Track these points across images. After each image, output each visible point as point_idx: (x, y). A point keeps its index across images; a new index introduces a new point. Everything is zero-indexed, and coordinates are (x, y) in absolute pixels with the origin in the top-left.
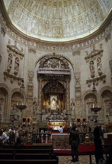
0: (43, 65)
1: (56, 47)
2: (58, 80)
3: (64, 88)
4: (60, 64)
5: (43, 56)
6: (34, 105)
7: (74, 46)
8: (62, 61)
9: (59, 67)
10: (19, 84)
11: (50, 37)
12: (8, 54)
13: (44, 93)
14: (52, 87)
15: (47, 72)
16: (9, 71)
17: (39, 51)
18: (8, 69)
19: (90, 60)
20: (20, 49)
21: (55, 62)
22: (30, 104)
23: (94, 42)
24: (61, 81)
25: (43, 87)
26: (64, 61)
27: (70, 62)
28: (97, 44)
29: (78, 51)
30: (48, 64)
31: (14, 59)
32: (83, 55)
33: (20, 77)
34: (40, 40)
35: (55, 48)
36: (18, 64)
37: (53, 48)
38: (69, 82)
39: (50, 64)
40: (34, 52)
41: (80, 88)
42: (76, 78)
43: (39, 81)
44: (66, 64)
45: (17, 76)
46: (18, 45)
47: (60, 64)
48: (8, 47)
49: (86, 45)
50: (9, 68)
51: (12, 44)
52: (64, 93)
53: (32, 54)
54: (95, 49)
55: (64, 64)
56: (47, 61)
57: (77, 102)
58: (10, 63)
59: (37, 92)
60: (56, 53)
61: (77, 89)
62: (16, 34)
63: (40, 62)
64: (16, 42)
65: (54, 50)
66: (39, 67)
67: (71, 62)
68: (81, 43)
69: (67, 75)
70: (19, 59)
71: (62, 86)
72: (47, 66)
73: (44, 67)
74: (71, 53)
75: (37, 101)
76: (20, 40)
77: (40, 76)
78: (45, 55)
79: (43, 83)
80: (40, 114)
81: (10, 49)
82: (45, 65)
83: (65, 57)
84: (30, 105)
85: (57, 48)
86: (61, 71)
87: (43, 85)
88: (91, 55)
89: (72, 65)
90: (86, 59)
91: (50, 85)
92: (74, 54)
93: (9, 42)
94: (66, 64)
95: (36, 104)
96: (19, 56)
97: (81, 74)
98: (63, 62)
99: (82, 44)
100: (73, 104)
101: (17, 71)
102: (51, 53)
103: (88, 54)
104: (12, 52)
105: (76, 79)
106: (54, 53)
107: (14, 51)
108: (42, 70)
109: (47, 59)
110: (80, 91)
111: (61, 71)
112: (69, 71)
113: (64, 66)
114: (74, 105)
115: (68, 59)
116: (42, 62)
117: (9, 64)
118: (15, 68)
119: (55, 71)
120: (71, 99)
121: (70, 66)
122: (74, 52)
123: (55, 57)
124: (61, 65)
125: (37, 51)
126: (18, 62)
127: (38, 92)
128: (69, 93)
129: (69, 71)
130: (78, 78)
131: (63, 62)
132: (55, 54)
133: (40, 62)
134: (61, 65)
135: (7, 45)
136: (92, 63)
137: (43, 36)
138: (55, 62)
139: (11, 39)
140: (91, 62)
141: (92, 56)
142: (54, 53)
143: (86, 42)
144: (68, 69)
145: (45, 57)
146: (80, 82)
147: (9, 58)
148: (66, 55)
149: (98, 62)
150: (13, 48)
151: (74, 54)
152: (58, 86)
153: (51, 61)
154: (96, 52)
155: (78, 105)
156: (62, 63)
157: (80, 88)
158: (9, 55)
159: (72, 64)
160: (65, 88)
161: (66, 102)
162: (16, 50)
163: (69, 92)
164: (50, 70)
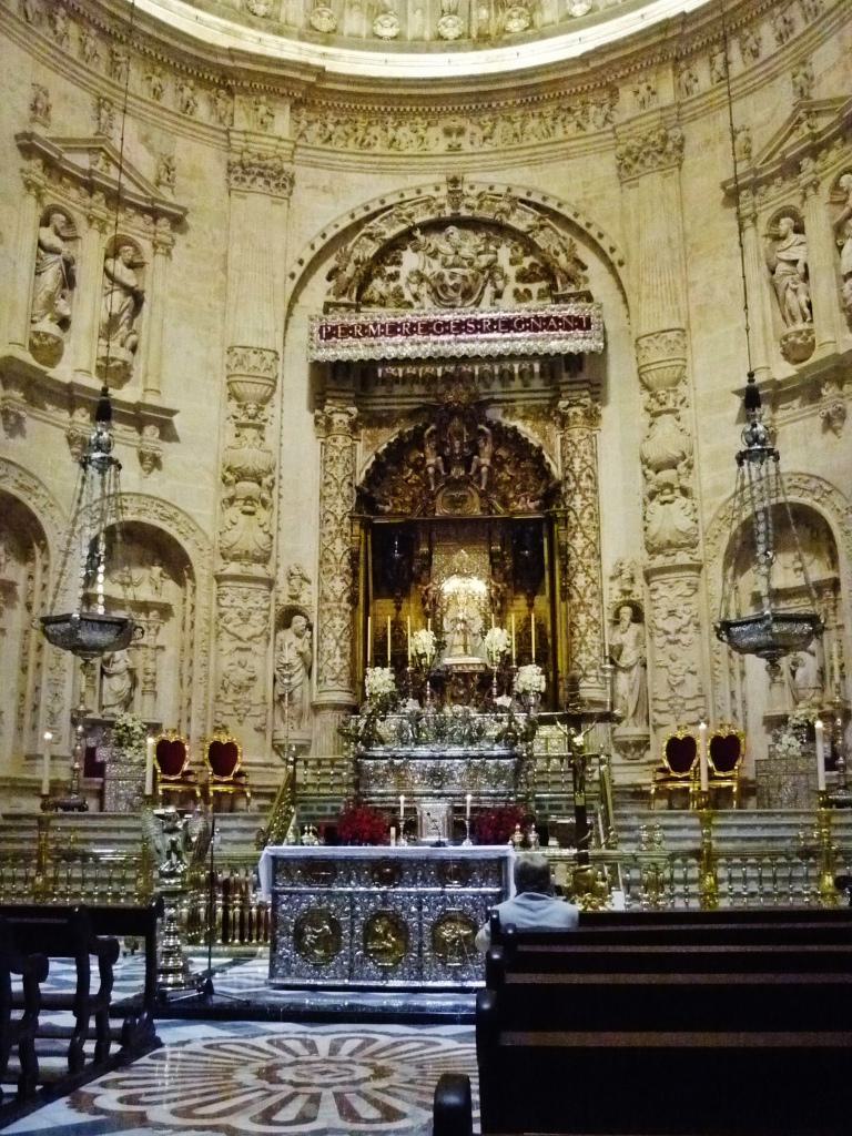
0: (362, 288)
1: (470, 128)
2: (494, 414)
3: (543, 472)
5: (361, 214)
6: (287, 636)
7: (626, 94)
8: (526, 242)
9: (498, 295)
10: (142, 457)
11: (417, 46)
12: (33, 212)
13: (367, 525)
14: (437, 470)
15: (391, 347)
16: (50, 351)
17: (325, 176)
18: (37, 334)
19: (779, 195)
20: (146, 165)
21: (466, 252)
22: (246, 620)
23: (800, 27)
24: (524, 418)
25: (360, 478)
26: (541, 240)
27: (594, 245)
28: (834, 39)
29: (665, 139)
30: (401, 282)
31: (90, 251)
32: (708, 168)
33: (151, 400)
34: (321, 73)
35: (461, 132)
36: (137, 298)
37: (448, 133)
38: (592, 417)
39: (422, 279)
40: (279, 180)
41: (690, 466)
42: (651, 378)
43: (326, 426)
44: (562, 259)
45: (127, 394)
46: (127, 136)
47: (511, 271)
48: (27, 146)
49: (737, 68)
50: (47, 326)
51: (72, 119)
52: (551, 521)
53: (257, 202)
54: (820, 93)
55: (547, 272)
56: (390, 250)
57: (663, 590)
58: (51, 277)
59: (315, 521)
60: (470, 177)
61: (667, 475)
62: (104, 34)
63: (331, 263)
64: (101, 103)
65: (454, 149)
66: (326, 311)
67: (604, 244)
68: (690, 56)
69: (574, 362)
70: (137, 250)
71: (529, 458)
72: (398, 294)
73: (369, 303)
74: (604, 166)
75: (309, 598)
76: (146, 95)
77: (331, 380)
78: (375, 207)
79: (360, 446)
80: (336, 707)
81: (50, 165)
82: (378, 286)
83: (551, 204)
84: (245, 635)
85: (477, 129)
86: (508, 325)
87: (364, 460)
88: (778, 156)
89: (610, 265)
90: (732, 195)
91: (424, 460)
92: (629, 165)
93: (39, 109)
94: (562, 259)
95: (299, 621)
96: (73, 193)
97: (698, 339)
98: (530, 247)
99: (703, 75)
100: (626, 612)
101: (123, 354)
102: (430, 182)
103: (754, 154)
104: (72, 199)
105: (647, 387)
106: (454, 181)
107: (91, 187)
108: (348, 331)
109: (390, 234)
110: (685, 492)
111: (508, 325)
113: (543, 285)
114: (638, 616)
115: (581, 222)
116: (351, 269)
117: (42, 297)
118: (111, 325)
119: (461, 327)
120: (608, 568)
121: (597, 279)
122: (629, 153)
123: (464, 212)
124: (522, 277)
126: (128, 277)
127: (324, 521)
128: (595, 516)
129: (581, 324)
130: (669, 375)
131: (530, 247)
132: (466, 189)
133: (331, 263)
134: (522, 277)
135: (17, 137)
136: (786, 224)
137: (356, 43)
138: (466, 252)
139: (58, 85)
140: (776, 221)
141: (792, 168)
142: (454, 181)
143: (734, 45)
144: (572, 309)
145: (375, 215)
146: (683, 412)
147: (40, 245)
148: (557, 183)
149: (837, 208)
150: (82, 161)
151: (629, 165)
152: (497, 463)
153: (434, 255)
154: (822, 123)
155: (672, 613)
156: (527, 262)
157: (681, 465)
158: (45, 222)
159: (614, 258)
160: (557, 472)
161: (566, 596)
162: (114, 173)
163: (595, 504)
164: (413, 328)
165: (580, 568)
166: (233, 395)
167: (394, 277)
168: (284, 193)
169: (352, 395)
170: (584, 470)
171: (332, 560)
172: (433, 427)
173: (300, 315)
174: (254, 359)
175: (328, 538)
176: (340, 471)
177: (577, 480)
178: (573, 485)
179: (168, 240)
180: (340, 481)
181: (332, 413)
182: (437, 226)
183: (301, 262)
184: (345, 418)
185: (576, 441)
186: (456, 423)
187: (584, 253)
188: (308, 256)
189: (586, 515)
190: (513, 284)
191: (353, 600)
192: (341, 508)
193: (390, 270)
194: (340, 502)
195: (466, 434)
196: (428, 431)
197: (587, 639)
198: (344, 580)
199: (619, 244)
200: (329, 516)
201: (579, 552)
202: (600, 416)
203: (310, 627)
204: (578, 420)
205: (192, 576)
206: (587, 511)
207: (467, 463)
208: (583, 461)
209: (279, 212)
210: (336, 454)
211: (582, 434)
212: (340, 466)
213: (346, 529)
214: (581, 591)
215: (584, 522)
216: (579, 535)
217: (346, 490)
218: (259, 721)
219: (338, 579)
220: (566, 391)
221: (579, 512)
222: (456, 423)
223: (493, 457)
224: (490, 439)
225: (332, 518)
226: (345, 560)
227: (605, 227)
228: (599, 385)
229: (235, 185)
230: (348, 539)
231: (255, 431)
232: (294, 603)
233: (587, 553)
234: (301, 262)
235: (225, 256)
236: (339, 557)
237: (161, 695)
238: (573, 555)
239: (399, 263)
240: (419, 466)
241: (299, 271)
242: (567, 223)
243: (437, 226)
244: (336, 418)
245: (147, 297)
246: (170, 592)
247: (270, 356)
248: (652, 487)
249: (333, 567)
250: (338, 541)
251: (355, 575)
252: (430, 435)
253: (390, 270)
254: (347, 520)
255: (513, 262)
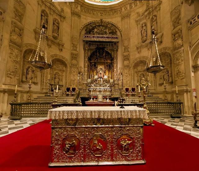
2: (106, 49)
4: (108, 32)
17: (85, 17)
38: (117, 50)
41: (129, 56)
44: (114, 31)
47: (108, 32)
67: (119, 29)
75: (83, 70)
79: (89, 53)
100: (120, 74)
112: (117, 38)
115: (117, 26)
123: (102, 24)
125: (82, 16)
129: (117, 38)
133: (85, 29)
152: (106, 56)
156: (110, 31)
160: (113, 57)
166: (72, 44)
167: (94, 32)
168: (79, 18)
173: (82, 35)
174: (75, 39)
179: (63, 20)
182: (99, 26)
183: (82, 28)
187: (117, 30)
188: (83, 27)
190: (108, 34)
191: (88, 71)
192: (86, 59)
193: (93, 31)
199: (121, 28)
203: (82, 74)
205: (67, 66)
207: (102, 55)
209: (79, 20)
218: (76, 85)
223: (105, 55)
227: (119, 26)
229: (73, 15)
234: (82, 28)
235: (71, 25)
237: (63, 81)
239: (94, 30)
240: (97, 55)
241: (81, 29)
242: (115, 26)
243: (99, 26)
244: (86, 48)
245: (60, 27)
246: (64, 68)
247: (77, 39)
251: (88, 68)
253: (93, 31)
255: (108, 31)
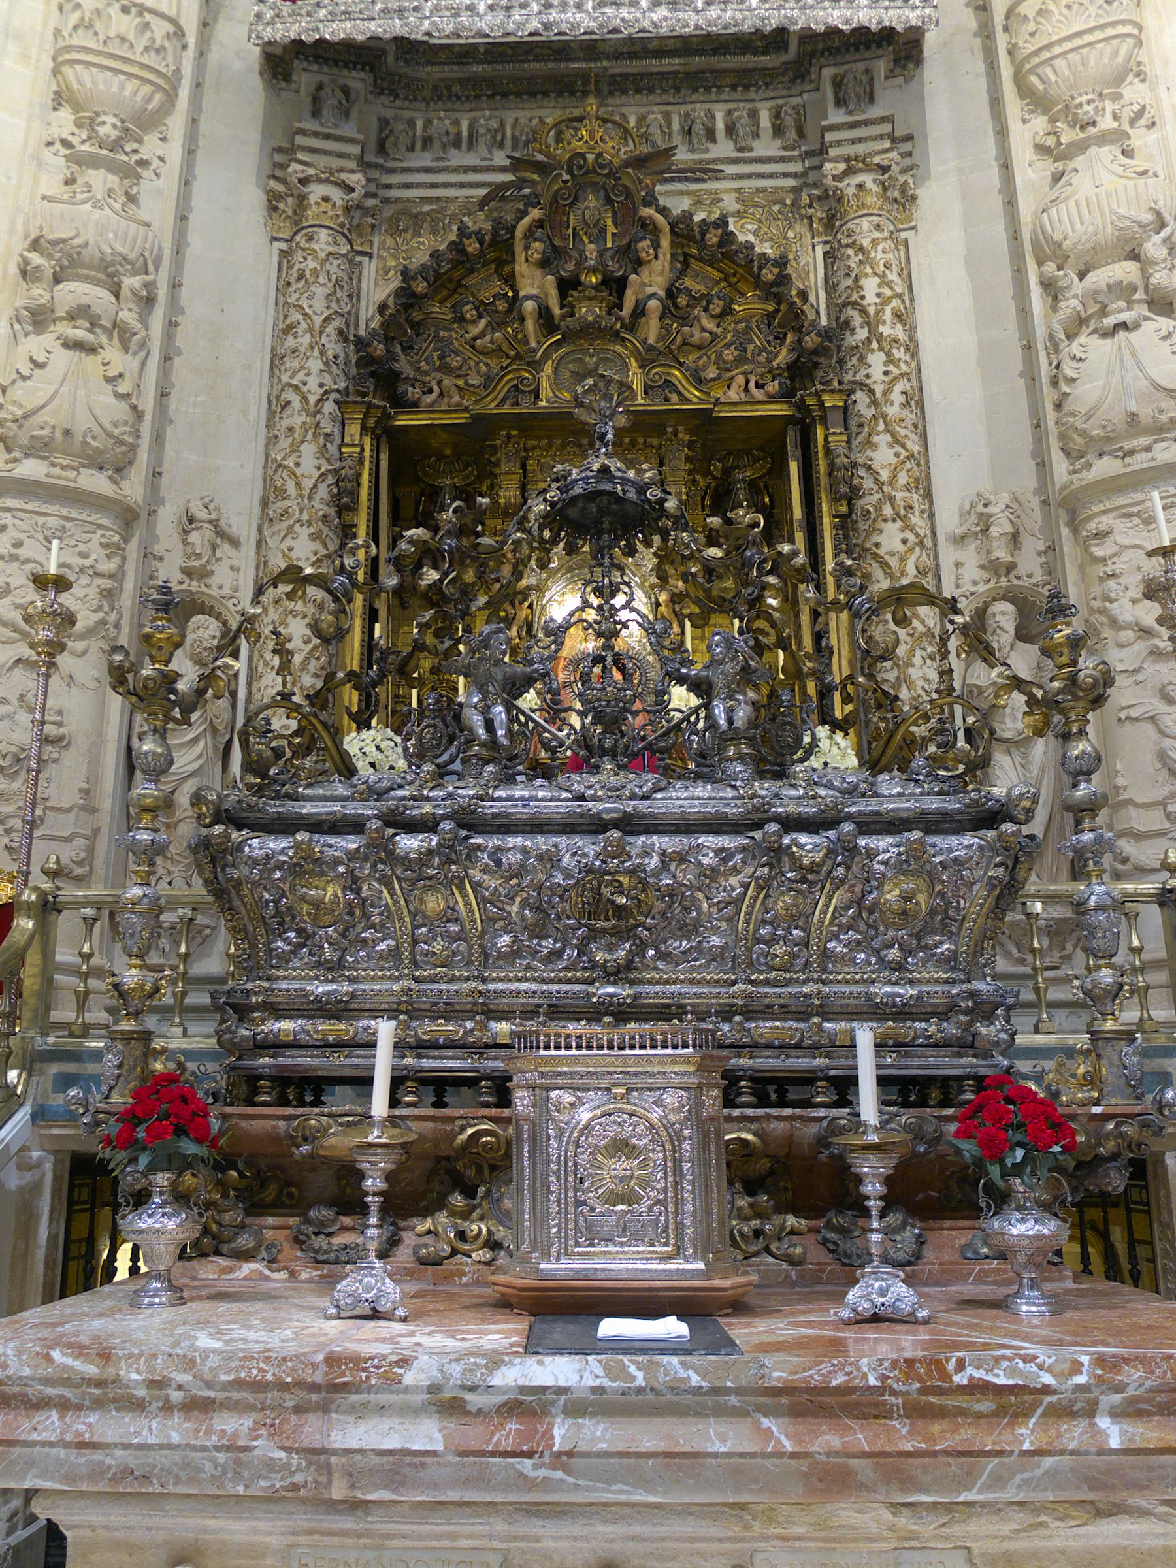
127: (277, 406)
165: (888, 510)
169: (355, 150)
170: (887, 301)
171: (292, 490)
172: (535, 214)
175: (284, 443)
176: (319, 304)
177: (871, 324)
178: (862, 334)
180: (318, 320)
181: (304, 181)
184: (336, 195)
185: (866, 243)
186: (591, 202)
189: (897, 397)
194: (315, 364)
195: (611, 229)
196: (526, 221)
197: (914, 673)
198: (314, 537)
200: (290, 395)
201: (884, 475)
202: (914, 198)
204: (870, 200)
206: (899, 387)
207: (615, 286)
208: (885, 283)
210: (312, 264)
211: (878, 227)
212: (320, 292)
213: (328, 426)
214: (893, 562)
215: (893, 411)
216: (882, 439)
217: (333, 347)
219: (304, 532)
220: (839, 143)
221: (879, 390)
222: (591, 202)
224: (665, 242)
225: (295, 399)
226: (323, 492)
228: (909, 138)
230: (332, 449)
231: (113, 180)
232: (194, 586)
233: (903, 478)
236: (308, 484)
238: (868, 483)
244: (316, 192)
248: (1070, 305)
249: (292, 504)
250: (309, 450)
252: (529, 235)
254: (329, 407)
